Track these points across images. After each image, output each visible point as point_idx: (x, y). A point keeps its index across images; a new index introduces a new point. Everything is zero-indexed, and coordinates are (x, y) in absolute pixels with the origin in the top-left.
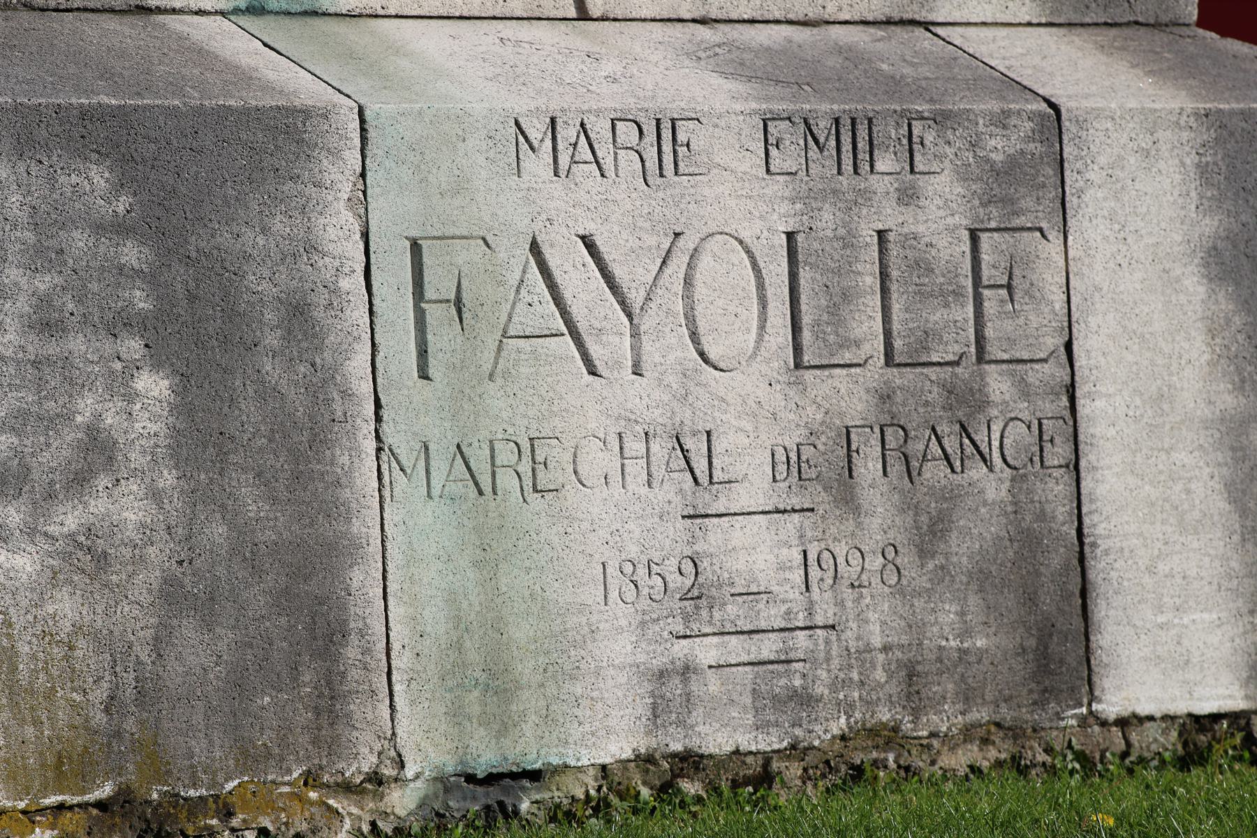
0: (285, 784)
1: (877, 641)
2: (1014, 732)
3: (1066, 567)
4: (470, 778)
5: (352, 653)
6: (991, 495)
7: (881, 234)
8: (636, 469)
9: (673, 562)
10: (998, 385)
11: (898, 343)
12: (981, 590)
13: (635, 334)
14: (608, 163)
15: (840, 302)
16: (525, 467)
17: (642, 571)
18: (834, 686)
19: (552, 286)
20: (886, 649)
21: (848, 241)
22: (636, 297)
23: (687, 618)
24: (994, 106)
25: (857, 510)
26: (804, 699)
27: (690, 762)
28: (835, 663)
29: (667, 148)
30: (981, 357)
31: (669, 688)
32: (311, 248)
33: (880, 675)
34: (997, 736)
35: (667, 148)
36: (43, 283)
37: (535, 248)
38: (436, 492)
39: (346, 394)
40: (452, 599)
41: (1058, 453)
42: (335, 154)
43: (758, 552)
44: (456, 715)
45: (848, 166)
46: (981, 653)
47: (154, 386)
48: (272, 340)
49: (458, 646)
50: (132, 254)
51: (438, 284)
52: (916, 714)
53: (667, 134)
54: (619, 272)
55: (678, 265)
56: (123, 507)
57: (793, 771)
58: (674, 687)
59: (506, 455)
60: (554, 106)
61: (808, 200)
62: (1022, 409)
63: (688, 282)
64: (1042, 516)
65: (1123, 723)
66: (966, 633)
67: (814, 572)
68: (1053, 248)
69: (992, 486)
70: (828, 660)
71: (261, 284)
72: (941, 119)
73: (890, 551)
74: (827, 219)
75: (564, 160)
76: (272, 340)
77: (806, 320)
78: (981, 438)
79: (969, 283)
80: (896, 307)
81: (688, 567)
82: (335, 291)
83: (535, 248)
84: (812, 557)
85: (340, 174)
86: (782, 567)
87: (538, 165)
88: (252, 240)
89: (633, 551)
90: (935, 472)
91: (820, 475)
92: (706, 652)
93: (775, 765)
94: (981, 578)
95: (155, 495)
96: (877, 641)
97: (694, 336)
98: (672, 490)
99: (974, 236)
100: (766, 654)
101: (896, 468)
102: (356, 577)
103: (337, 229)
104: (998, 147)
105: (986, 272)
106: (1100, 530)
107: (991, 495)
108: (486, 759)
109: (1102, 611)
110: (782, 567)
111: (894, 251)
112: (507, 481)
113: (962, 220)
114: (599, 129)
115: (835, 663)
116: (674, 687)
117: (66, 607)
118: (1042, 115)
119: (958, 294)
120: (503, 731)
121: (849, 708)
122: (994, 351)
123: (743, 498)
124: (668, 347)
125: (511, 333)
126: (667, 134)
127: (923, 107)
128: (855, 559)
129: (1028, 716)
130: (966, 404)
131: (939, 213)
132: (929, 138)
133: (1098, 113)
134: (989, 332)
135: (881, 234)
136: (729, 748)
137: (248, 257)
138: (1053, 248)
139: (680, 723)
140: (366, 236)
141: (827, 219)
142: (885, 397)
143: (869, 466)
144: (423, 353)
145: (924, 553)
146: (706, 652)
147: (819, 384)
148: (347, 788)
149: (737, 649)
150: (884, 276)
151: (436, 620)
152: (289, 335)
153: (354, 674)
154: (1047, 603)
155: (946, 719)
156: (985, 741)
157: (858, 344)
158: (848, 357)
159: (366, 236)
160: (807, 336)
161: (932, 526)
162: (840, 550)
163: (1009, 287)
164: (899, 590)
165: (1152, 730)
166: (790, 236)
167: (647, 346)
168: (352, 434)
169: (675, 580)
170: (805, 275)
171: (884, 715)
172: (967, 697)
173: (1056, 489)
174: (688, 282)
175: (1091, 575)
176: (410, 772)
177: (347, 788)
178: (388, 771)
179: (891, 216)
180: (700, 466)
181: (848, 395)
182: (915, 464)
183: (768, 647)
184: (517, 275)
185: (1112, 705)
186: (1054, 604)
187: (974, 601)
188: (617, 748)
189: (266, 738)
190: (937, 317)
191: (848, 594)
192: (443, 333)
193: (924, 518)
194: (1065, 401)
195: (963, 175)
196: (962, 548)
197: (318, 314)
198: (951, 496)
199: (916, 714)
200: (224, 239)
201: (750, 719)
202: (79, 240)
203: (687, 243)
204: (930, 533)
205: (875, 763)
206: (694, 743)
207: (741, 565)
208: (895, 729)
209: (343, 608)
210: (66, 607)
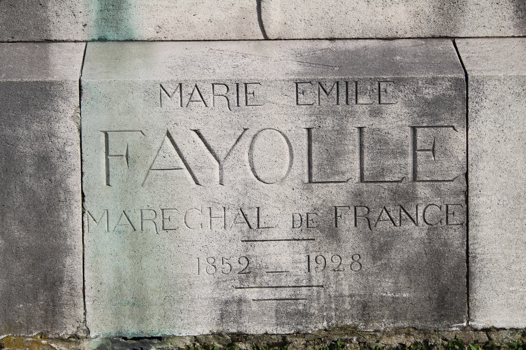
0: (29, 337)
1: (346, 293)
2: (424, 331)
3: (458, 267)
4: (126, 339)
5: (65, 289)
6: (416, 235)
7: (361, 129)
8: (218, 223)
9: (236, 259)
10: (423, 191)
11: (366, 173)
12: (407, 273)
13: (221, 169)
14: (210, 102)
15: (334, 156)
16: (159, 220)
17: (218, 263)
18: (321, 310)
19: (177, 150)
20: (351, 296)
21: (341, 132)
22: (222, 155)
23: (241, 281)
24: (430, 75)
25: (339, 240)
26: (305, 315)
27: (240, 337)
28: (322, 301)
29: (242, 95)
30: (415, 179)
31: (229, 308)
32: (52, 135)
33: (347, 306)
34: (415, 333)
35: (242, 95)
37: (168, 135)
38: (112, 228)
39: (67, 191)
40: (117, 270)
41: (458, 218)
42: (65, 99)
43: (283, 256)
44: (117, 314)
46: (405, 300)
48: (30, 170)
49: (120, 288)
51: (116, 148)
52: (366, 322)
53: (242, 89)
54: (211, 144)
55: (246, 141)
57: (300, 342)
58: (234, 308)
59: (148, 215)
60: (181, 79)
61: (319, 115)
62: (437, 201)
63: (251, 148)
64: (445, 244)
65: (487, 330)
66: (397, 290)
67: (313, 264)
68: (461, 135)
69: (418, 232)
70: (318, 299)
71: (25, 148)
72: (397, 82)
73: (356, 258)
74: (329, 123)
75: (185, 100)
76: (30, 170)
77: (315, 163)
78: (412, 212)
79: (410, 149)
80: (366, 159)
81: (244, 261)
82: (64, 152)
83: (168, 135)
84: (312, 258)
85: (68, 108)
86: (295, 262)
87: (172, 103)
88: (21, 132)
89: (214, 254)
90: (385, 226)
91: (321, 227)
92: (252, 294)
93: (289, 339)
94: (408, 268)
96: (346, 293)
97: (253, 170)
98: (237, 231)
99: (414, 129)
100: (284, 296)
101: (362, 223)
102: (68, 261)
103: (66, 128)
104: (429, 93)
105: (419, 145)
106: (479, 251)
107: (416, 235)
109: (476, 284)
110: (295, 262)
111: (366, 135)
112: (149, 226)
113: (407, 123)
114: (206, 88)
115: (322, 301)
116: (234, 308)
118: (457, 80)
119: (403, 153)
120: (142, 320)
121: (329, 319)
122: (421, 176)
123: (275, 234)
124: (239, 173)
125: (153, 168)
126: (242, 89)
127: (388, 77)
128: (337, 260)
129: (430, 325)
131: (395, 118)
132: (390, 89)
133: (490, 78)
134: (420, 169)
135: (361, 129)
136: (262, 332)
137: (18, 139)
139: (235, 321)
140: (80, 130)
141: (329, 123)
143: (347, 222)
144: (108, 176)
145: (375, 258)
146: (252, 294)
147: (320, 190)
148: (62, 340)
149: (268, 293)
150: (361, 145)
151: (109, 278)
152: (38, 169)
153: (65, 297)
154: (444, 280)
155: (385, 324)
156: (408, 334)
157: (343, 173)
158: (337, 178)
159: (80, 130)
160: (314, 170)
161: (381, 249)
162: (328, 256)
163: (433, 151)
164: (360, 272)
165: (504, 334)
166: (309, 130)
167: (226, 173)
168: (69, 206)
169: (236, 265)
170: (315, 146)
171: (349, 322)
172: (396, 318)
174: (251, 148)
175: (472, 269)
176: (92, 335)
177: (62, 340)
178: (81, 334)
179: (366, 122)
180: (253, 221)
181: (337, 194)
182: (373, 222)
183: (285, 293)
184: (158, 145)
185: (480, 323)
186: (451, 281)
187: (402, 278)
188: (203, 329)
189: (21, 320)
190: (390, 162)
191: (332, 274)
192: (119, 168)
193: (377, 244)
194: (462, 197)
195: (408, 104)
196: (397, 256)
197: (54, 160)
198: (394, 236)
199: (366, 322)
200: (8, 131)
201: (274, 321)
203: (251, 133)
204: (380, 250)
205: (346, 341)
206: (243, 329)
207: (273, 260)
208: (355, 328)
209: (61, 271)
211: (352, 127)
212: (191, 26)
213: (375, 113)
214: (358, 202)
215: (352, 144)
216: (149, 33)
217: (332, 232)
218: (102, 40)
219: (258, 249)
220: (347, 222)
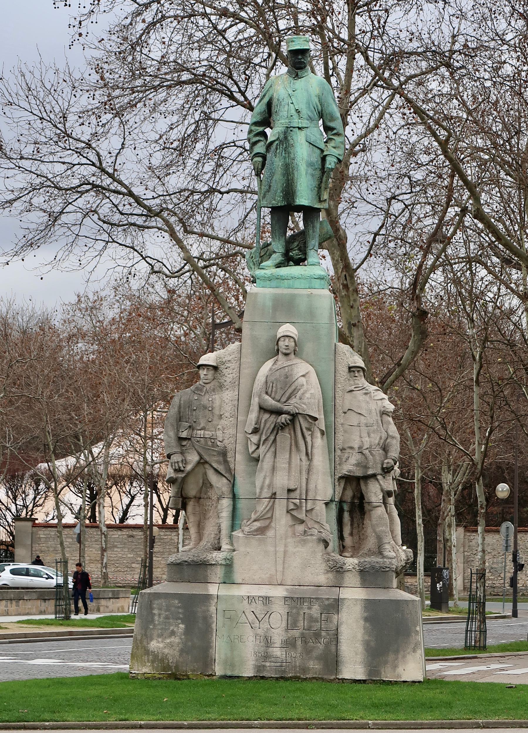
10: (323, 634)
36: (167, 613)
45: (299, 603)
47: (182, 626)
50: (180, 611)
69: (321, 647)
95: (181, 639)
111: (306, 615)
119: (318, 622)
130: (317, 635)
138: (336, 616)
143: (299, 643)
173: (333, 648)
179: (306, 611)
195: (320, 606)
202: (173, 609)
211: (302, 613)
212: (254, 580)
213: (310, 608)
214: (303, 636)
215: (301, 618)
216: (240, 581)
218: (224, 583)
219: (271, 649)
220: (299, 643)
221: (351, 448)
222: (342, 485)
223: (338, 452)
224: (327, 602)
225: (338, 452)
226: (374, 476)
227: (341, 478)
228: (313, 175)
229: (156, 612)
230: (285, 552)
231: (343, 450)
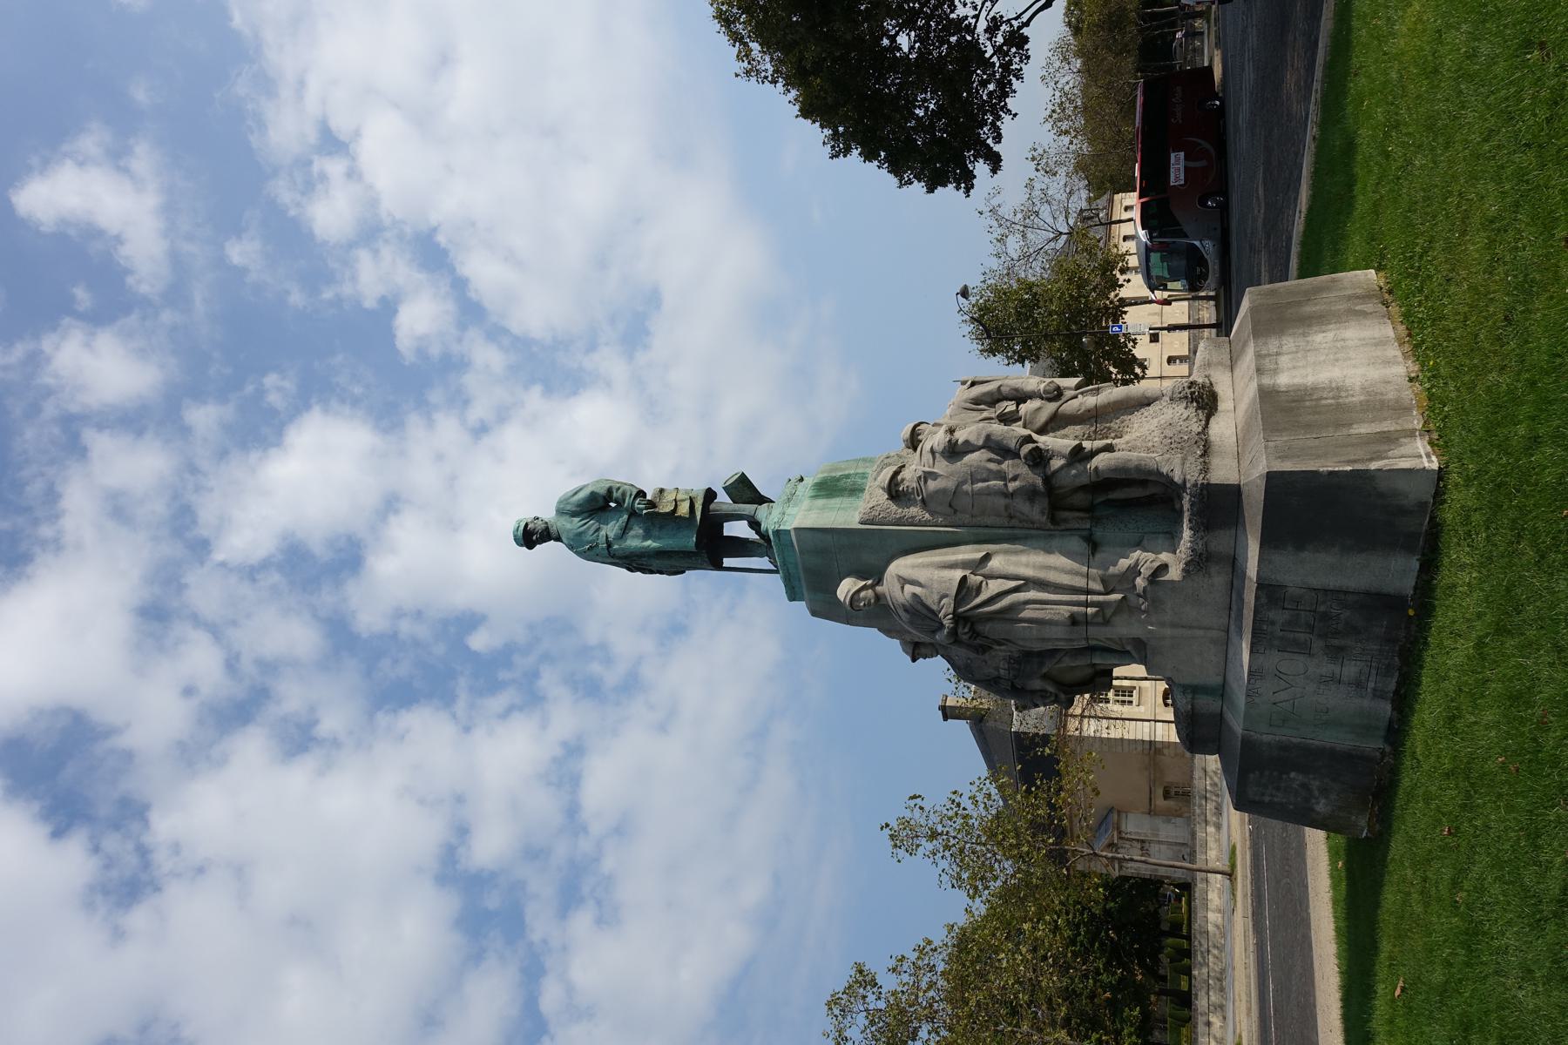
10: (1322, 608)
31: (1378, 694)
43: (1351, 670)
56: (1315, 784)
69: (1346, 614)
85: (1256, 736)
91: (1337, 653)
103: (1266, 738)
108: (1383, 733)
117: (1333, 797)
130: (1325, 617)
138: (1290, 590)
141: (1276, 642)
142: (1320, 636)
143: (1336, 642)
146: (1371, 685)
149: (1372, 678)
188: (1389, 707)
210: (1333, 797)
213: (1273, 623)
215: (1291, 635)
217: (1341, 649)
219: (1344, 678)
221: (1007, 507)
222: (1066, 514)
223: (1014, 522)
224: (1264, 600)
225: (1014, 522)
226: (1047, 480)
227: (1053, 519)
228: (661, 528)
229: (1267, 799)
230: (1174, 625)
231: (1011, 517)
